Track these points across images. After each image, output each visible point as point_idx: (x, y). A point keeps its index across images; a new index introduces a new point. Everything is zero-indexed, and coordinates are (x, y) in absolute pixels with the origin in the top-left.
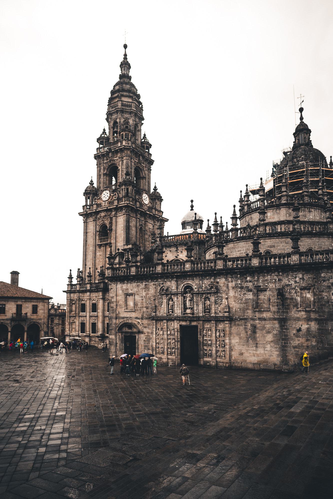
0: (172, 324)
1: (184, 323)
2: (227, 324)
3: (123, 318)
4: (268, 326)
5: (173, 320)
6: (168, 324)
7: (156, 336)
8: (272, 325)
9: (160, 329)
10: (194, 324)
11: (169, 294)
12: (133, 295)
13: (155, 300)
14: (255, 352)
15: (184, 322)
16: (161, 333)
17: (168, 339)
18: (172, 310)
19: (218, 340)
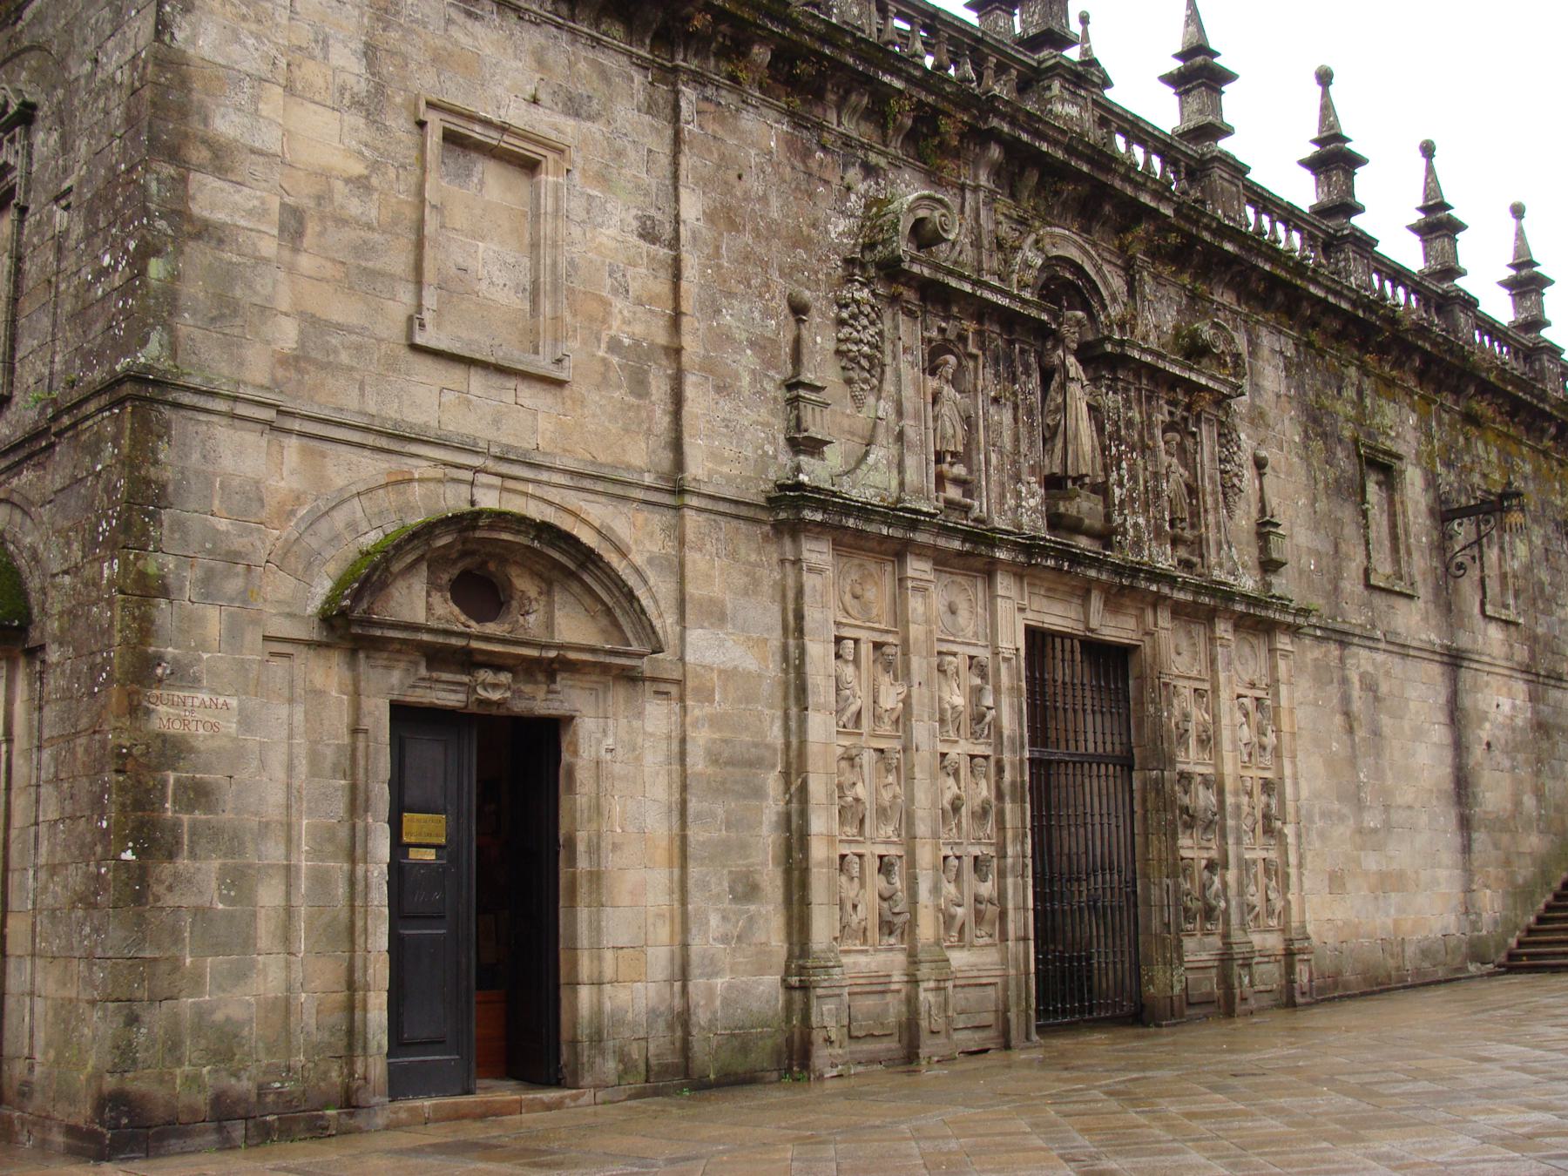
1: (1059, 616)
9: (866, 649)
10: (1115, 628)
12: (530, 166)
15: (1058, 608)
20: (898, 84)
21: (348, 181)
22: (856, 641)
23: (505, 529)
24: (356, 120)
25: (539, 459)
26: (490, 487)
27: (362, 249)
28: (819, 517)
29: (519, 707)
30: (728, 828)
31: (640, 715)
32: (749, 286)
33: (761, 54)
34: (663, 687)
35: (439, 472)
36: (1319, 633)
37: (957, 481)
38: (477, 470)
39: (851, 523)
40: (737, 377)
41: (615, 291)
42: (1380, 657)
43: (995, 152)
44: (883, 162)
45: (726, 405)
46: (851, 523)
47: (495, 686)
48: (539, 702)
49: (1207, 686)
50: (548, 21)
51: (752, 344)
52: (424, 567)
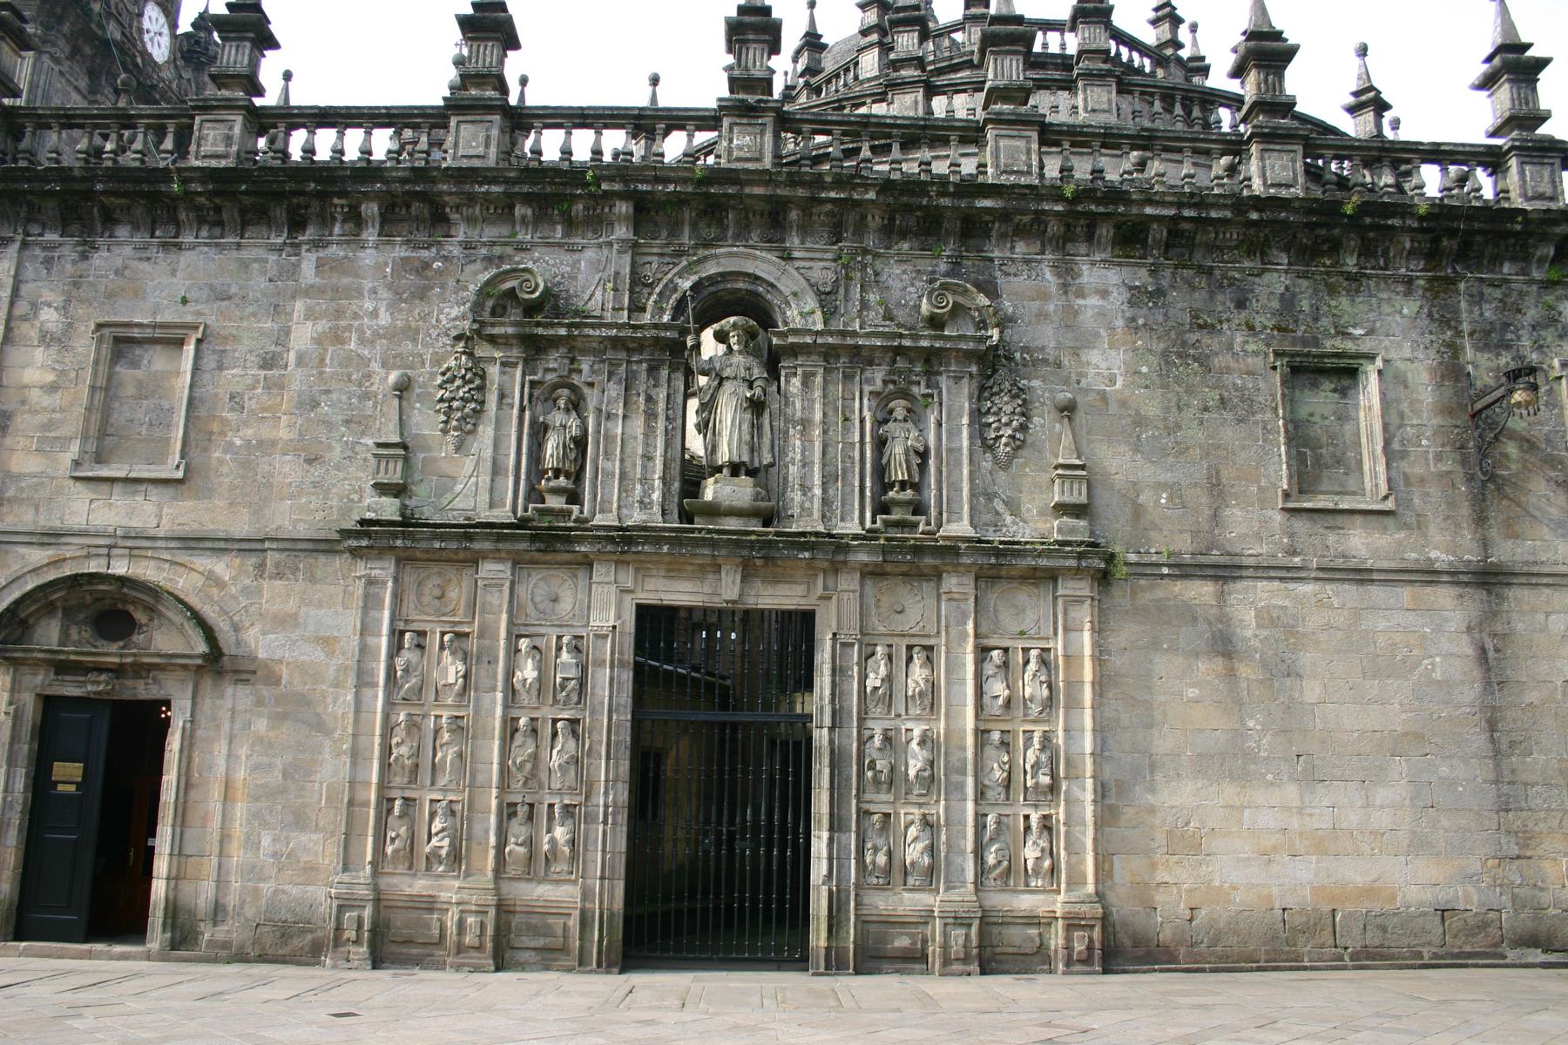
0: (555, 600)
1: (681, 592)
2: (1078, 600)
3: (51, 537)
4: (1382, 624)
5: (587, 564)
6: (522, 591)
7: (390, 704)
8: (1411, 616)
11: (554, 342)
12: (180, 343)
13: (403, 389)
14: (1295, 823)
16: (452, 670)
17: (510, 729)
18: (567, 477)
19: (996, 736)
20: (495, 189)
21: (42, 388)
22: (422, 634)
23: (103, 583)
24: (54, 350)
25: (152, 533)
26: (122, 556)
27: (49, 426)
28: (364, 543)
29: (127, 695)
30: (285, 774)
31: (222, 696)
32: (350, 380)
33: (371, 209)
34: (244, 676)
35: (84, 552)
36: (1165, 571)
37: (556, 491)
38: (110, 547)
39: (399, 543)
40: (330, 448)
41: (232, 410)
42: (1308, 588)
43: (623, 208)
44: (509, 250)
45: (317, 472)
46: (399, 543)
47: (99, 683)
48: (143, 690)
49: (931, 642)
50: (199, 244)
51: (347, 422)
52: (60, 614)
